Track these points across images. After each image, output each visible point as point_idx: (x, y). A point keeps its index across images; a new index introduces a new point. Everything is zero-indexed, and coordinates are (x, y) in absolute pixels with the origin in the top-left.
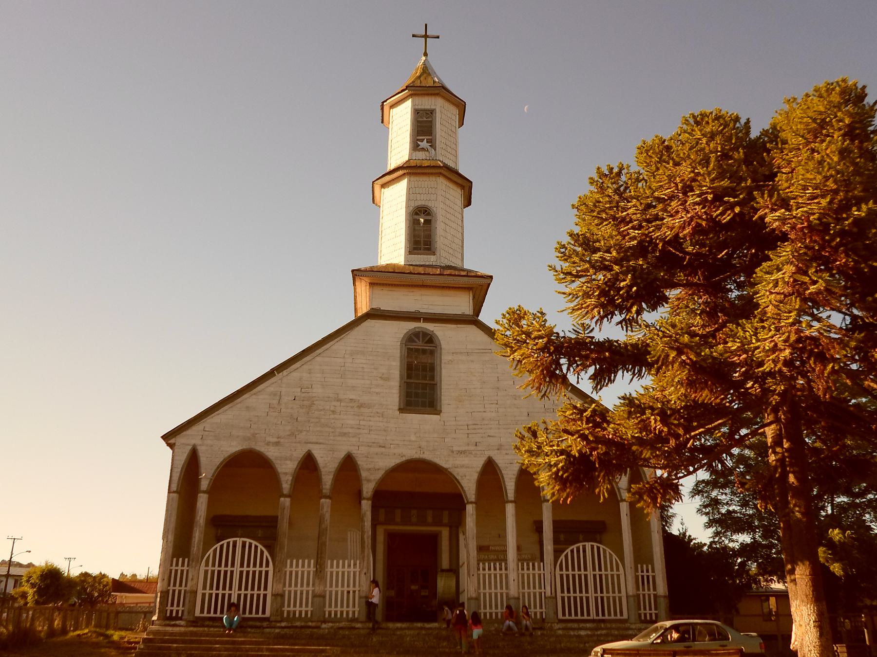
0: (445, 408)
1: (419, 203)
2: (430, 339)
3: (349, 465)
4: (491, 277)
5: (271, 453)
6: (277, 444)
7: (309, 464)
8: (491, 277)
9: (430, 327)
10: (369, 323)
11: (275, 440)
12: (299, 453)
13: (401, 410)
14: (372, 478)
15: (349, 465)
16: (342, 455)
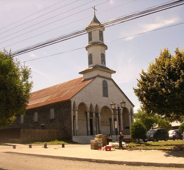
0: (109, 96)
1: (102, 53)
2: (106, 82)
3: (97, 106)
4: (116, 72)
5: (86, 103)
6: (87, 101)
7: (91, 105)
8: (116, 72)
9: (106, 80)
10: (98, 78)
11: (86, 101)
12: (90, 104)
13: (103, 96)
14: (100, 109)
15: (97, 106)
16: (96, 105)
